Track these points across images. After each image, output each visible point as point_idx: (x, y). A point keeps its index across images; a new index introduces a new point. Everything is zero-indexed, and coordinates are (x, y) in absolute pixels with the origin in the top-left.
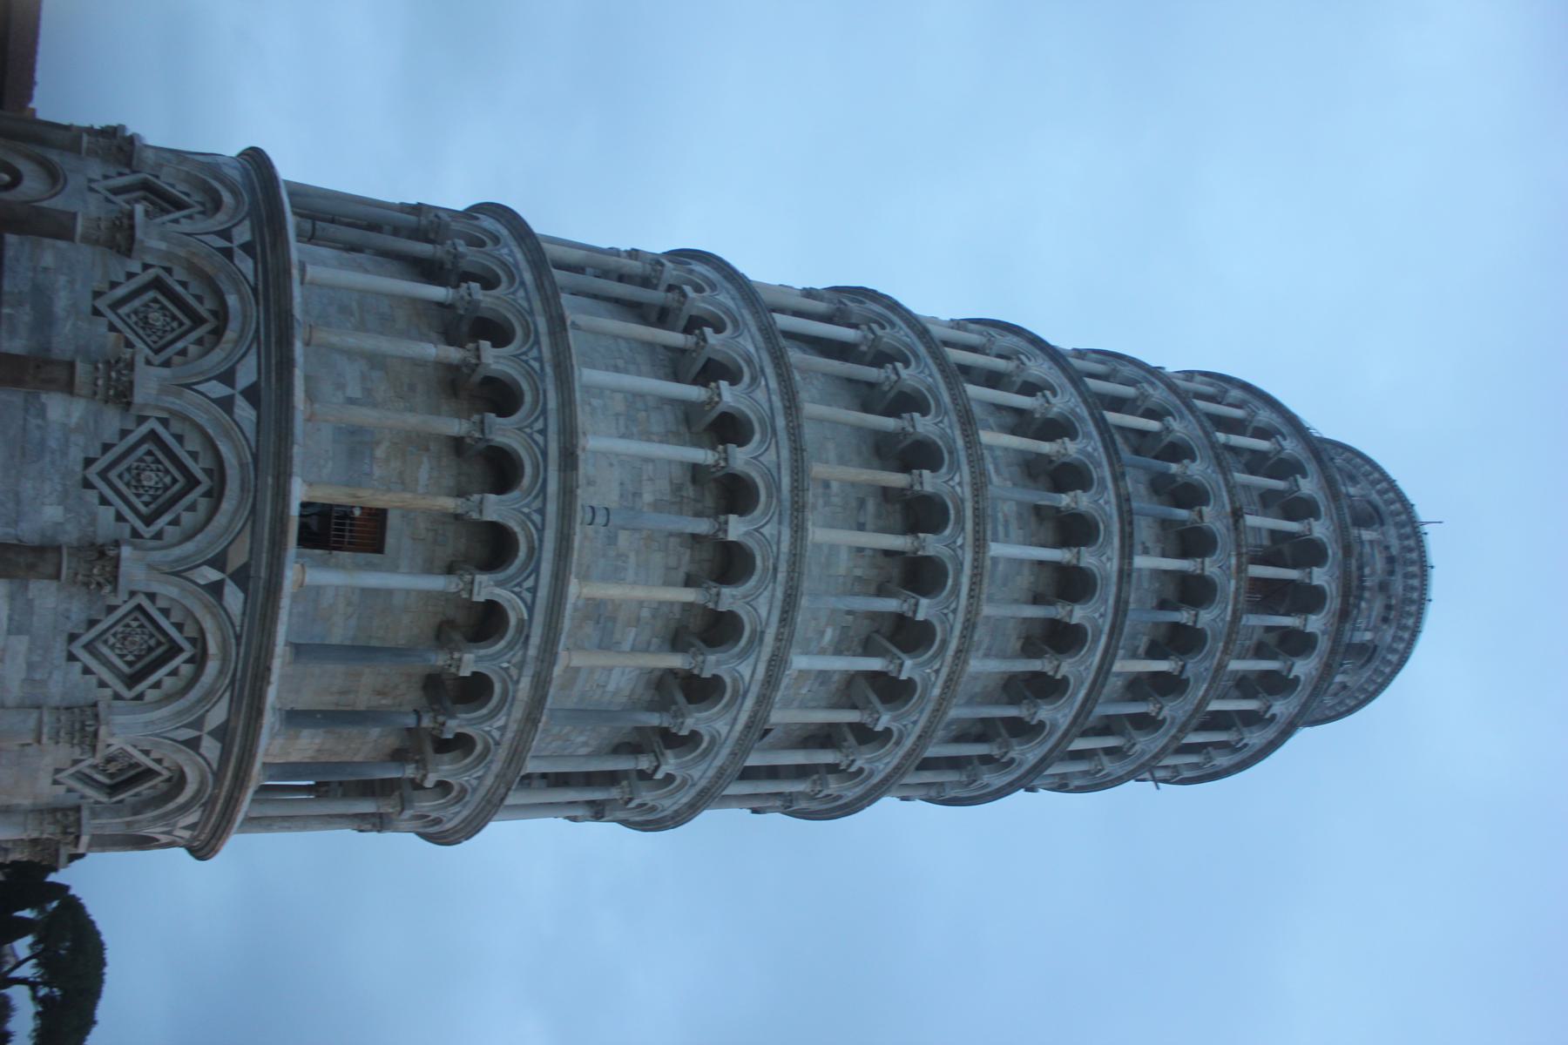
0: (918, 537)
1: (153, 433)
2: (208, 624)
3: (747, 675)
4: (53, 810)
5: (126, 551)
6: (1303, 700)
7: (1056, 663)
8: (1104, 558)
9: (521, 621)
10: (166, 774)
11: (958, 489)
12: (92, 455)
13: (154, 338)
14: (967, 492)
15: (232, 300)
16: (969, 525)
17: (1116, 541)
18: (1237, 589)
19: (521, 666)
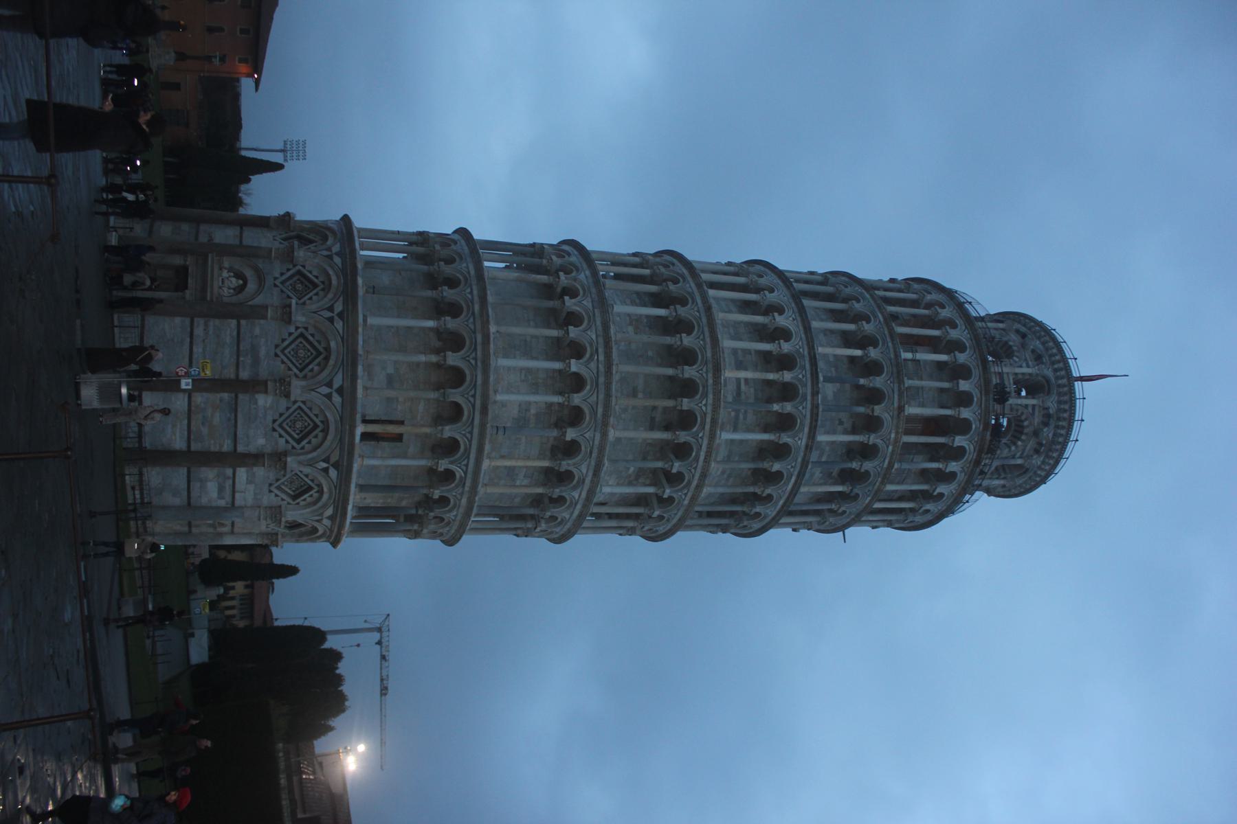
0: (675, 433)
2: (324, 482)
4: (268, 534)
5: (289, 459)
6: (948, 504)
7: (762, 489)
8: (797, 439)
9: (461, 477)
10: (310, 526)
11: (704, 408)
12: (275, 418)
13: (300, 362)
14: (710, 408)
15: (333, 344)
16: (707, 427)
17: (806, 430)
18: (893, 451)
19: (462, 494)
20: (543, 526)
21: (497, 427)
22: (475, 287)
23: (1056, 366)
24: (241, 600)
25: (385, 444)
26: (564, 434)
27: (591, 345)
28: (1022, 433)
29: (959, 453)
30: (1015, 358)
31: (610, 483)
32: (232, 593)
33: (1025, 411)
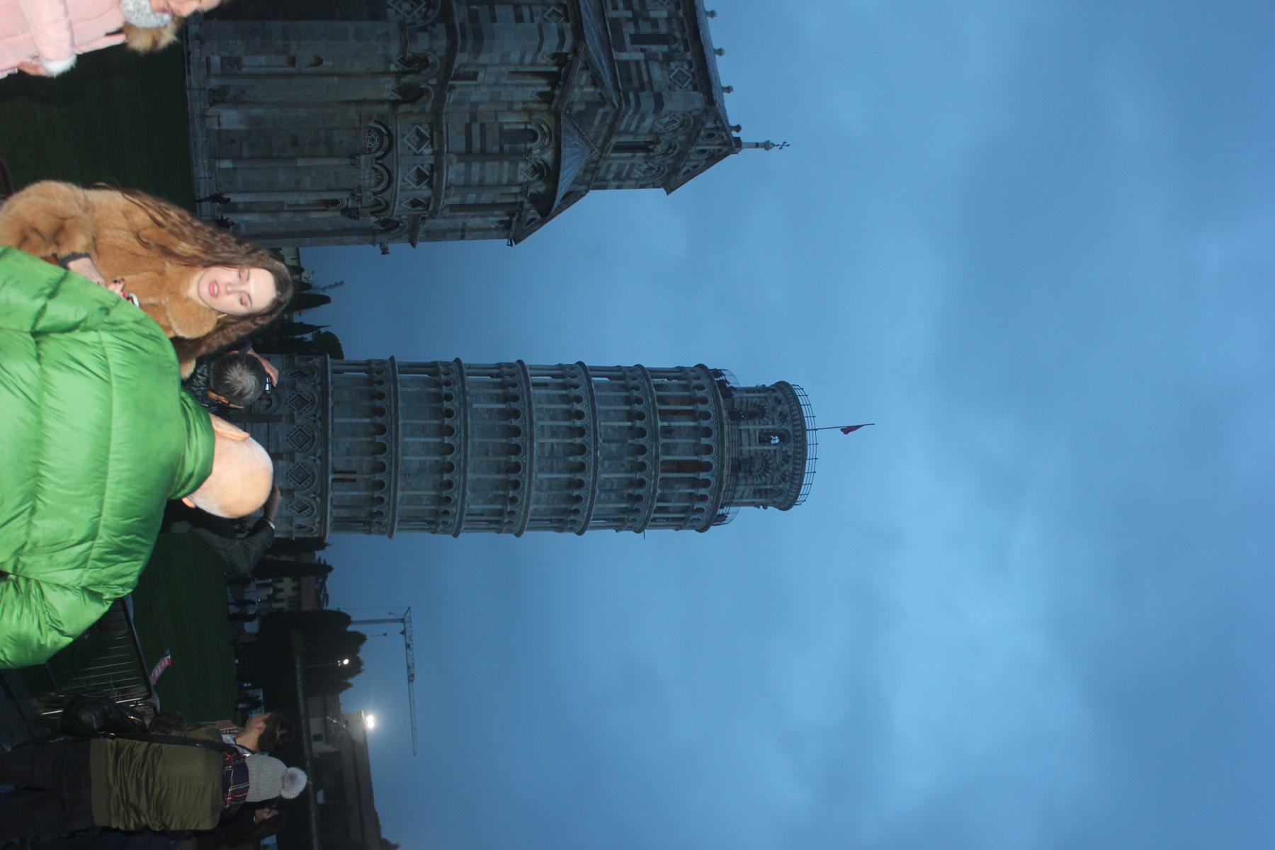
1: (300, 467)
3: (455, 511)
5: (295, 493)
14: (528, 461)
15: (316, 434)
16: (527, 471)
17: (592, 472)
20: (441, 527)
21: (405, 475)
22: (392, 399)
23: (795, 423)
24: (289, 602)
25: (346, 483)
26: (442, 477)
27: (457, 428)
28: (768, 468)
29: (706, 483)
30: (765, 419)
31: (480, 502)
32: (280, 596)
33: (769, 454)
